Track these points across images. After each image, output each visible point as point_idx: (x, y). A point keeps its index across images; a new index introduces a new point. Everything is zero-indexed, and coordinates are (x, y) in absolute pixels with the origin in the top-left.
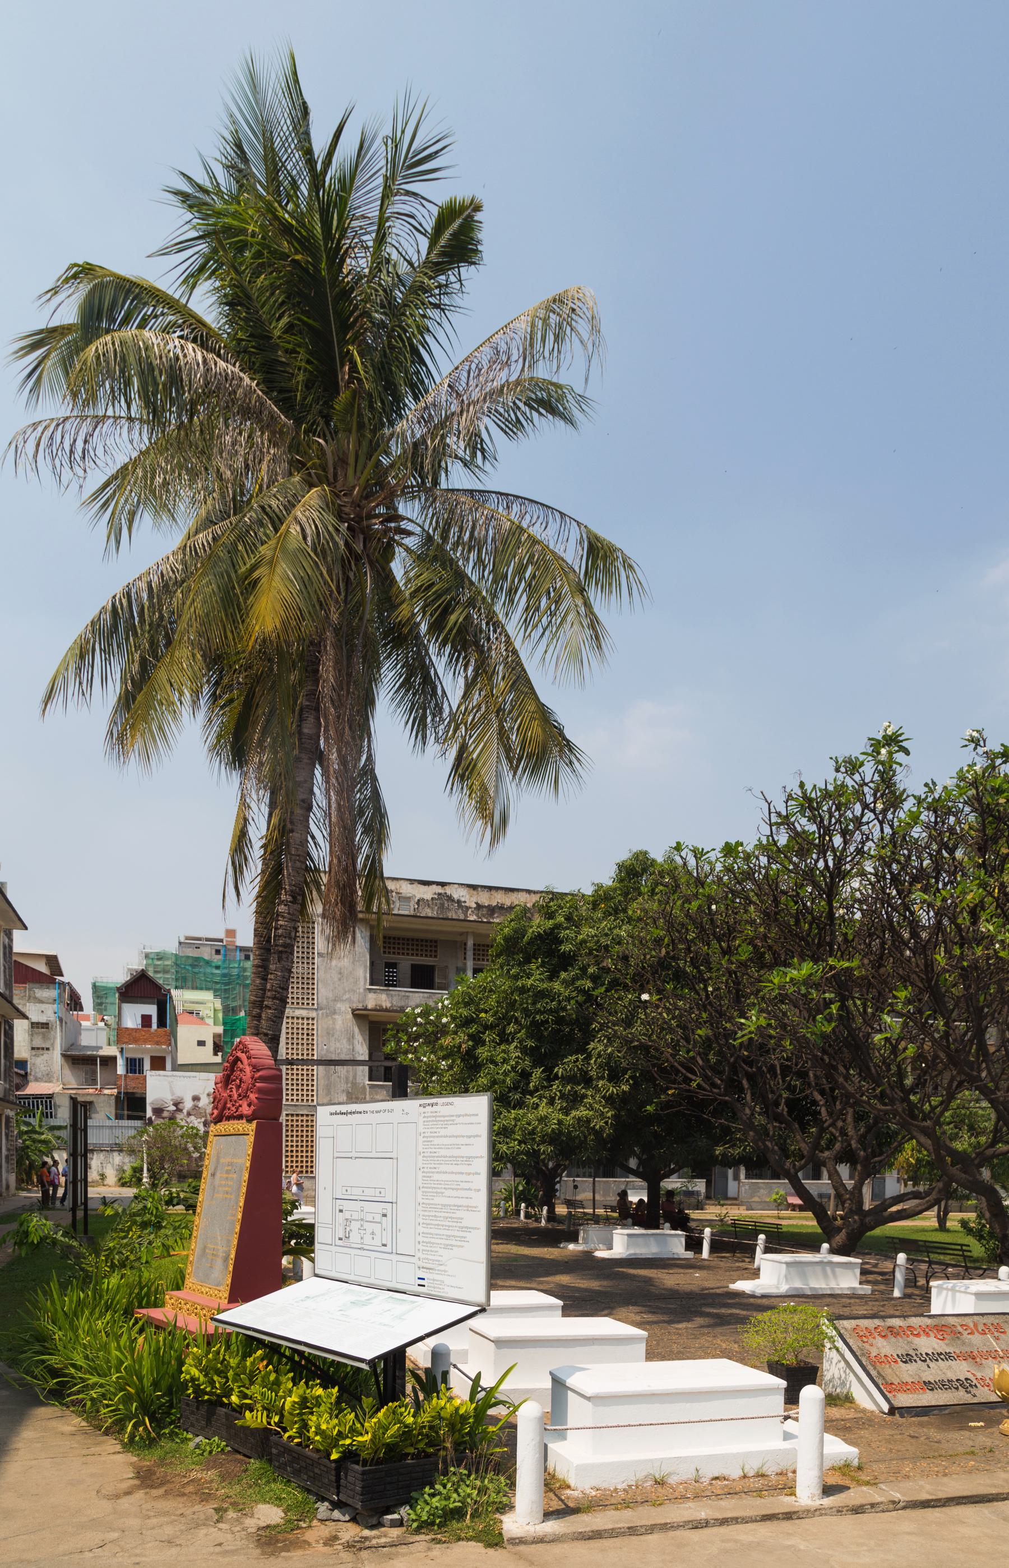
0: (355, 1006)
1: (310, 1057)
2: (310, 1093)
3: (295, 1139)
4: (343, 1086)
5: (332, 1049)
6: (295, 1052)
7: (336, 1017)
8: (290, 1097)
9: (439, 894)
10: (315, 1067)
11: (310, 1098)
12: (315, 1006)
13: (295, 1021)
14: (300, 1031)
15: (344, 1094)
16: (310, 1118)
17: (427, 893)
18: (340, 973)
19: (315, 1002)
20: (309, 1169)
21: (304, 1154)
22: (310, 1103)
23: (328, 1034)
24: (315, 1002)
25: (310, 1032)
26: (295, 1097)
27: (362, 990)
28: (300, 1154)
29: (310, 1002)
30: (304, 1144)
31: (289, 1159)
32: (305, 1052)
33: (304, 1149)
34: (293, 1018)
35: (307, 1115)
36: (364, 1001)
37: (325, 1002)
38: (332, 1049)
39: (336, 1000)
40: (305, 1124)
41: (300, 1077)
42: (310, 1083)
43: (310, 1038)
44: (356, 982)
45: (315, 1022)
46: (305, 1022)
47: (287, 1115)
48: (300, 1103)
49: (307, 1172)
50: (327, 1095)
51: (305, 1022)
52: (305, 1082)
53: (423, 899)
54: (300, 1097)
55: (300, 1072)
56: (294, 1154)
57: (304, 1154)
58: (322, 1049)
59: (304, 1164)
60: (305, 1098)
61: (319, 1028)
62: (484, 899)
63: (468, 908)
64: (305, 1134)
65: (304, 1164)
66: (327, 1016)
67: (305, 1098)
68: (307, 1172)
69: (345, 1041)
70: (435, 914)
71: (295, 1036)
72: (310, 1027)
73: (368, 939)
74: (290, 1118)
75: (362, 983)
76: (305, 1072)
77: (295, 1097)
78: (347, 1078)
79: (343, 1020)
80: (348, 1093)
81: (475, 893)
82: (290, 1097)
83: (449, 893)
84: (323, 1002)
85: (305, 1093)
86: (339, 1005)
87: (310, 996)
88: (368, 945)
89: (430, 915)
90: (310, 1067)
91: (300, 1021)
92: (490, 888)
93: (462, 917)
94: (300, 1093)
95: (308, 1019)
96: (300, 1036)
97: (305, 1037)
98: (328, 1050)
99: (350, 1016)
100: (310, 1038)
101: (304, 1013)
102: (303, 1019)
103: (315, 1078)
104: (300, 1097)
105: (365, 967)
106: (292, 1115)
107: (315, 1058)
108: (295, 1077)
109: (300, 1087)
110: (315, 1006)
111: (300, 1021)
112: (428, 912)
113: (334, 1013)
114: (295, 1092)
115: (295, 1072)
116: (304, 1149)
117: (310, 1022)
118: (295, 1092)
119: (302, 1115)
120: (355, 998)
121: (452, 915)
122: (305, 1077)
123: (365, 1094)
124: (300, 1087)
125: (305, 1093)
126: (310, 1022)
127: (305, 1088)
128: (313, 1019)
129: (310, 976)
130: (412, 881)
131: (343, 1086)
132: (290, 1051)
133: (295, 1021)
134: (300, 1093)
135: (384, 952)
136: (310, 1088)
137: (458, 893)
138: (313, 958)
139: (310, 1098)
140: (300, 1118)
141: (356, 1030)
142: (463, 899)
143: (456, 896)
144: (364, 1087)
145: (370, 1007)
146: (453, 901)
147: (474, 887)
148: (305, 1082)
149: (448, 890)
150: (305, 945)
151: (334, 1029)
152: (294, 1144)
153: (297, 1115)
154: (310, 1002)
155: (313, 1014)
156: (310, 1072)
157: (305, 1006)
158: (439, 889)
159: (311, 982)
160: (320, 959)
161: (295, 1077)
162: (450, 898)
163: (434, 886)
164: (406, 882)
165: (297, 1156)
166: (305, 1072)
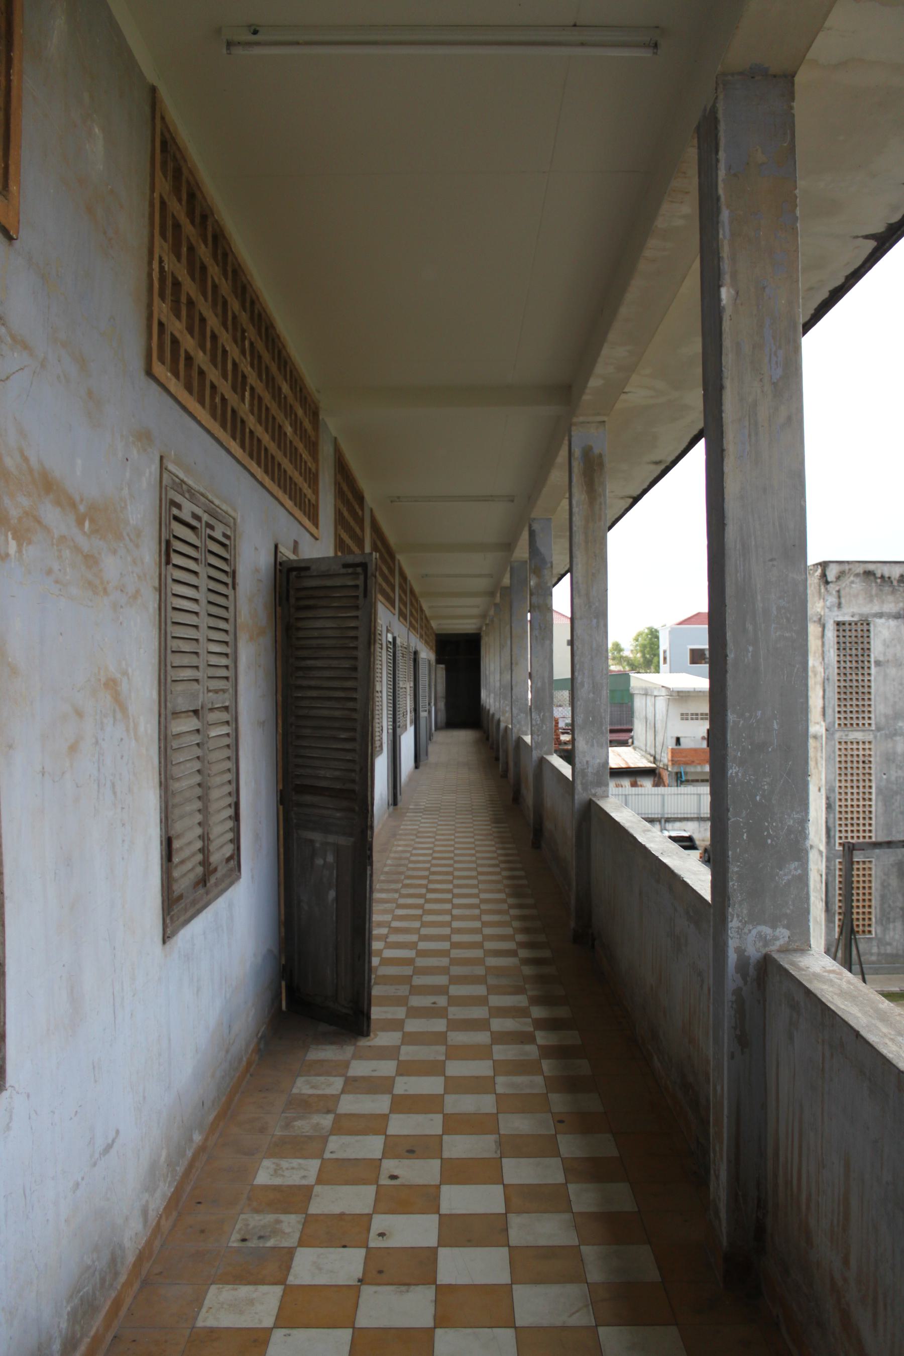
7: (898, 738)
12: (873, 727)
13: (849, 746)
16: (867, 866)
19: (872, 722)
24: (872, 722)
25: (867, 759)
29: (867, 722)
35: (864, 862)
37: (883, 720)
38: (893, 778)
46: (861, 746)
51: (861, 746)
87: (866, 715)
91: (855, 746)
95: (864, 743)
96: (855, 765)
97: (861, 765)
98: (888, 780)
100: (867, 766)
103: (873, 816)
110: (873, 727)
117: (867, 746)
126: (867, 746)
128: (870, 742)
129: (866, 690)
136: (867, 828)
138: (869, 668)
150: (860, 652)
151: (895, 753)
154: (867, 722)
155: (870, 737)
159: (866, 697)
160: (878, 668)
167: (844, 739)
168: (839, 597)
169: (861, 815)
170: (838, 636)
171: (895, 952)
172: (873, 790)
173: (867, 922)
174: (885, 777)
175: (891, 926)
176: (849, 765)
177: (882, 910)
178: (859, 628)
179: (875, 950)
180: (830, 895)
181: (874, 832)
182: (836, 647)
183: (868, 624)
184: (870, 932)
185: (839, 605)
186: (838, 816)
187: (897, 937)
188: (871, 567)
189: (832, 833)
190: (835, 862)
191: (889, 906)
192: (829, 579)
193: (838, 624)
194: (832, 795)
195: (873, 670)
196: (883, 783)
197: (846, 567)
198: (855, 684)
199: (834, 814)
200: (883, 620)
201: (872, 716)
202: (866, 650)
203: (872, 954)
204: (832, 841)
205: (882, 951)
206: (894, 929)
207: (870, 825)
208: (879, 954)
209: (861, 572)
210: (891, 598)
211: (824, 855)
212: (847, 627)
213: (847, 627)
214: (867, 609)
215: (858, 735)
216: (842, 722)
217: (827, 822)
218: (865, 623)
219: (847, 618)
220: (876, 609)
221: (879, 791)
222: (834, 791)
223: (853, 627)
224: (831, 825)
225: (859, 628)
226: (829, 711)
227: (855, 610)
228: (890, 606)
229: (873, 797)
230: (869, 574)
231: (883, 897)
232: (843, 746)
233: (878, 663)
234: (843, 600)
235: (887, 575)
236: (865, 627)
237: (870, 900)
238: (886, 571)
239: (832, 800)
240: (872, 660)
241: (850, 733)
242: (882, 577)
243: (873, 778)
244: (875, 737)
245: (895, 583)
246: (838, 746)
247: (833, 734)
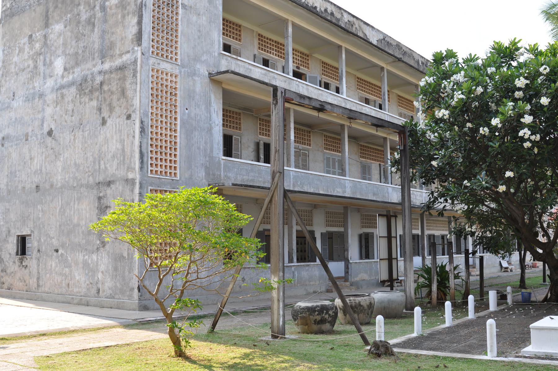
5: (193, 115)
15: (203, 169)
18: (199, 31)
27: (216, 54)
37: (186, 59)
39: (197, 59)
42: (173, 152)
43: (174, 98)
60: (168, 170)
69: (203, 107)
99: (207, 80)
103: (178, 147)
155: (177, 72)
167: (156, 67)
172: (178, 122)
174: (187, 111)
181: (178, 162)
186: (150, 142)
189: (145, 159)
190: (147, 189)
194: (145, 119)
195: (180, 11)
196: (186, 117)
199: (147, 139)
201: (179, 52)
204: (145, 166)
211: (137, 182)
215: (165, 66)
217: (141, 147)
221: (183, 123)
222: (147, 116)
224: (144, 150)
226: (145, 37)
229: (178, 128)
239: (145, 124)
241: (161, 63)
243: (178, 110)
244: (180, 72)
246: (151, 73)
247: (148, 59)
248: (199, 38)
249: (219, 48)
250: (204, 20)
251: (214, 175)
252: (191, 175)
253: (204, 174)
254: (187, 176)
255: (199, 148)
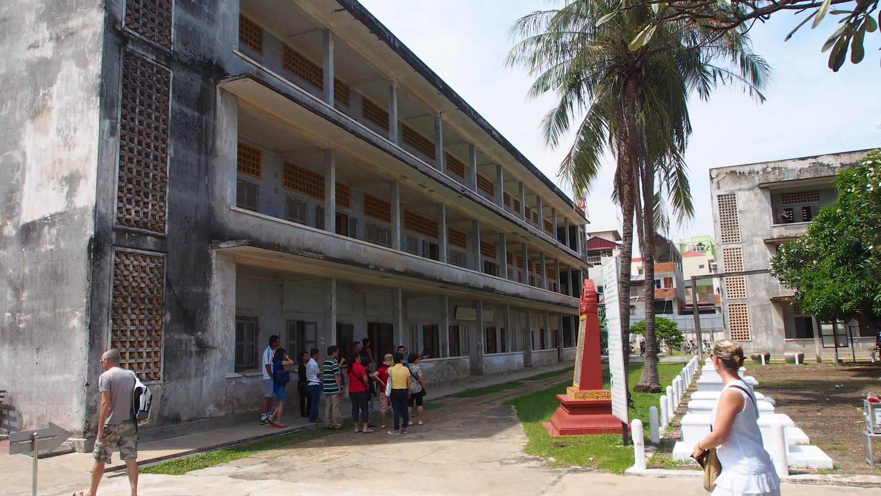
0: (765, 238)
1: (740, 271)
2: (742, 292)
3: (735, 319)
4: (763, 286)
5: (754, 264)
6: (730, 268)
7: (754, 245)
8: (730, 295)
9: (814, 163)
10: (744, 276)
11: (743, 294)
12: (740, 241)
13: (729, 251)
14: (733, 257)
16: (744, 306)
17: (805, 164)
20: (747, 337)
21: (742, 328)
22: (743, 297)
23: (750, 256)
25: (739, 256)
26: (733, 295)
27: (769, 228)
28: (739, 328)
29: (737, 239)
30: (742, 322)
31: (733, 331)
32: (737, 268)
33: (742, 325)
34: (727, 249)
35: (742, 305)
36: (771, 234)
37: (746, 238)
38: (754, 264)
39: (753, 235)
40: (741, 310)
41: (735, 283)
42: (742, 285)
43: (739, 259)
44: (765, 223)
45: (741, 250)
46: (735, 251)
47: (730, 305)
48: (736, 298)
49: (745, 338)
50: (753, 292)
51: (735, 251)
52: (739, 286)
53: (803, 168)
54: (736, 295)
55: (735, 280)
56: (736, 328)
57: (742, 328)
58: (747, 265)
59: (743, 334)
60: (739, 295)
61: (744, 253)
62: (846, 160)
63: (835, 168)
64: (741, 316)
65: (743, 334)
66: (748, 246)
67: (739, 295)
68: (745, 338)
69: (761, 259)
70: (812, 176)
71: (730, 260)
72: (738, 253)
73: (769, 198)
74: (731, 307)
75: (768, 224)
76: (738, 280)
77: (733, 295)
78: (765, 280)
79: (759, 247)
80: (767, 289)
81: (839, 157)
82: (730, 295)
83: (820, 161)
84: (745, 238)
85: (739, 292)
86: (755, 239)
88: (770, 202)
89: (809, 177)
90: (741, 277)
91: (732, 251)
92: (850, 153)
93: (832, 174)
94: (736, 292)
95: (737, 249)
96: (733, 259)
97: (736, 259)
100: (739, 259)
101: (734, 246)
102: (733, 249)
104: (736, 295)
105: (769, 214)
106: (733, 305)
107: (743, 271)
108: (732, 283)
109: (736, 289)
111: (732, 251)
112: (808, 175)
113: (753, 243)
114: (733, 292)
115: (732, 280)
116: (742, 325)
117: (738, 250)
118: (733, 292)
119: (739, 305)
120: (765, 233)
121: (824, 174)
122: (738, 283)
123: (778, 289)
124: (736, 289)
125: (739, 292)
126: (738, 250)
127: (739, 289)
128: (740, 249)
129: (735, 225)
130: (794, 160)
131: (763, 286)
132: (727, 269)
133: (729, 251)
134: (736, 292)
135: (783, 203)
137: (826, 161)
139: (743, 294)
140: (738, 307)
141: (768, 252)
142: (831, 163)
143: (825, 162)
144: (777, 284)
145: (775, 237)
146: (824, 165)
147: (838, 154)
148: (739, 286)
149: (820, 160)
151: (753, 253)
152: (736, 322)
153: (736, 305)
154: (737, 239)
155: (740, 246)
156: (741, 279)
157: (734, 242)
158: (813, 161)
160: (741, 214)
161: (732, 283)
162: (822, 164)
163: (810, 159)
164: (791, 161)
165: (738, 329)
166: (738, 280)
167: (726, 248)
168: (719, 184)
169: (738, 283)
170: (719, 202)
171: (763, 348)
173: (746, 334)
175: (760, 335)
176: (730, 260)
177: (754, 327)
178: (730, 197)
179: (752, 347)
180: (725, 320)
182: (718, 207)
183: (734, 195)
184: (748, 338)
185: (719, 188)
187: (764, 341)
188: (734, 169)
189: (724, 292)
191: (758, 325)
192: (713, 177)
193: (719, 196)
195: (738, 216)
197: (721, 170)
198: (729, 222)
200: (742, 192)
202: (734, 206)
203: (751, 349)
205: (756, 348)
206: (762, 337)
207: (743, 287)
208: (755, 349)
209: (729, 172)
210: (745, 182)
212: (724, 197)
213: (724, 197)
214: (732, 188)
216: (725, 240)
218: (732, 195)
219: (723, 193)
220: (738, 187)
223: (727, 197)
225: (730, 197)
227: (727, 189)
228: (745, 185)
230: (733, 173)
231: (754, 321)
232: (726, 251)
233: (740, 212)
234: (720, 185)
235: (742, 172)
236: (733, 196)
237: (747, 323)
238: (742, 170)
240: (737, 210)
242: (740, 173)
245: (747, 174)
248: (754, 224)
249: (770, 224)
250: (756, 213)
251: (773, 292)
252: (756, 295)
253: (765, 293)
254: (753, 295)
255: (760, 280)
